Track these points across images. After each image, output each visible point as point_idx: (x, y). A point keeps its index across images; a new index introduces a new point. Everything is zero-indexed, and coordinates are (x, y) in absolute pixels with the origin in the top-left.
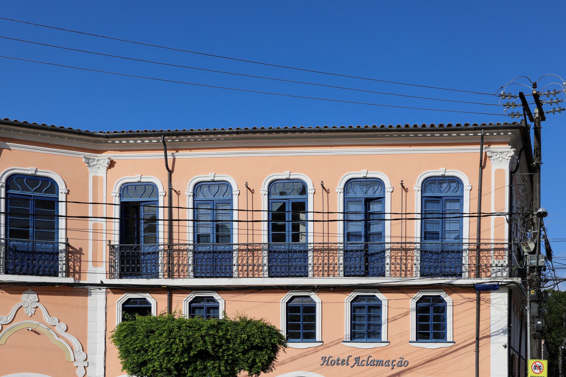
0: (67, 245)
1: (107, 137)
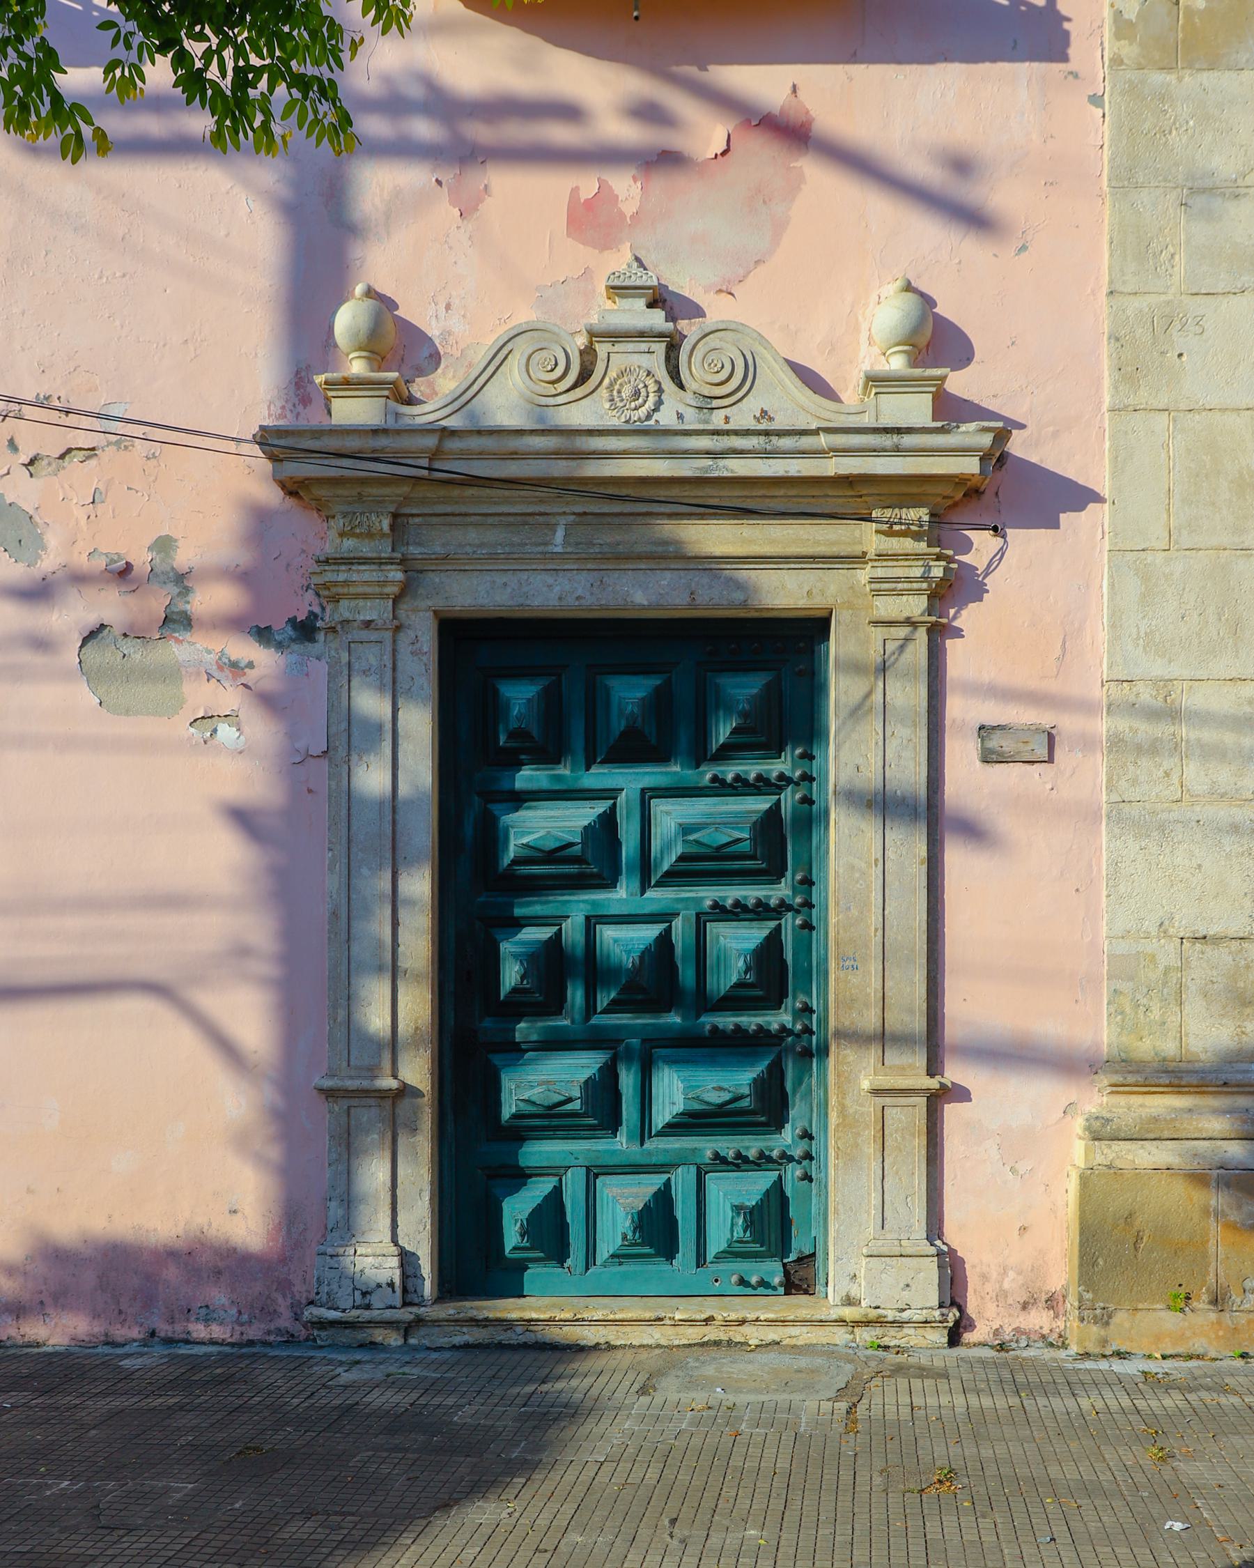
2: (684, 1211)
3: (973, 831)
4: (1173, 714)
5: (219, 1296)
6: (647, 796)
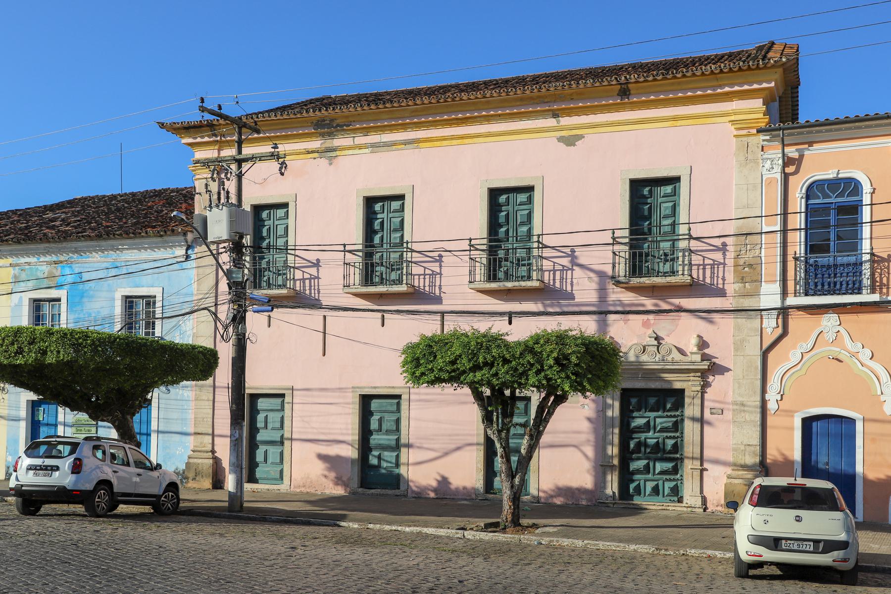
0: (872, 254)
6: (655, 418)
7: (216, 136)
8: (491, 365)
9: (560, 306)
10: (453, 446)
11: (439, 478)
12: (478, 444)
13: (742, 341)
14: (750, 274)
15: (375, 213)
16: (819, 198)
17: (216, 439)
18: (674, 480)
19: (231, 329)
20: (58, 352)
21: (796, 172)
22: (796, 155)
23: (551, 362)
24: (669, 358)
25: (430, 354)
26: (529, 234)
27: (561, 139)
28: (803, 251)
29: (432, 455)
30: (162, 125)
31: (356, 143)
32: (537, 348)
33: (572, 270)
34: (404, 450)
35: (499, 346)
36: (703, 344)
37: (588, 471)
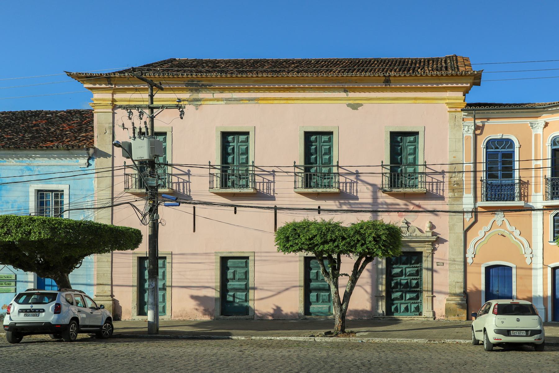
0: (520, 180)
1: (544, 108)
2: (409, 308)
3: (436, 271)
4: (455, 261)
5: (365, 315)
7: (111, 84)
8: (334, 241)
9: (350, 204)
10: (284, 288)
11: (275, 308)
12: (300, 286)
13: (454, 225)
14: (457, 188)
15: (229, 142)
16: (493, 148)
17: (114, 287)
18: (417, 303)
19: (147, 217)
20: (40, 233)
21: (481, 134)
22: (481, 124)
23: (371, 239)
24: (414, 235)
25: (296, 234)
26: (330, 160)
27: (349, 105)
28: (485, 176)
29: (270, 293)
30: (70, 74)
31: (215, 97)
32: (362, 231)
33: (357, 183)
34: (251, 292)
35: (339, 230)
36: (432, 227)
37: (368, 300)
